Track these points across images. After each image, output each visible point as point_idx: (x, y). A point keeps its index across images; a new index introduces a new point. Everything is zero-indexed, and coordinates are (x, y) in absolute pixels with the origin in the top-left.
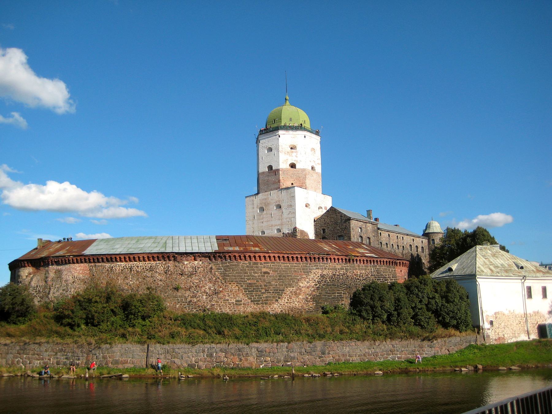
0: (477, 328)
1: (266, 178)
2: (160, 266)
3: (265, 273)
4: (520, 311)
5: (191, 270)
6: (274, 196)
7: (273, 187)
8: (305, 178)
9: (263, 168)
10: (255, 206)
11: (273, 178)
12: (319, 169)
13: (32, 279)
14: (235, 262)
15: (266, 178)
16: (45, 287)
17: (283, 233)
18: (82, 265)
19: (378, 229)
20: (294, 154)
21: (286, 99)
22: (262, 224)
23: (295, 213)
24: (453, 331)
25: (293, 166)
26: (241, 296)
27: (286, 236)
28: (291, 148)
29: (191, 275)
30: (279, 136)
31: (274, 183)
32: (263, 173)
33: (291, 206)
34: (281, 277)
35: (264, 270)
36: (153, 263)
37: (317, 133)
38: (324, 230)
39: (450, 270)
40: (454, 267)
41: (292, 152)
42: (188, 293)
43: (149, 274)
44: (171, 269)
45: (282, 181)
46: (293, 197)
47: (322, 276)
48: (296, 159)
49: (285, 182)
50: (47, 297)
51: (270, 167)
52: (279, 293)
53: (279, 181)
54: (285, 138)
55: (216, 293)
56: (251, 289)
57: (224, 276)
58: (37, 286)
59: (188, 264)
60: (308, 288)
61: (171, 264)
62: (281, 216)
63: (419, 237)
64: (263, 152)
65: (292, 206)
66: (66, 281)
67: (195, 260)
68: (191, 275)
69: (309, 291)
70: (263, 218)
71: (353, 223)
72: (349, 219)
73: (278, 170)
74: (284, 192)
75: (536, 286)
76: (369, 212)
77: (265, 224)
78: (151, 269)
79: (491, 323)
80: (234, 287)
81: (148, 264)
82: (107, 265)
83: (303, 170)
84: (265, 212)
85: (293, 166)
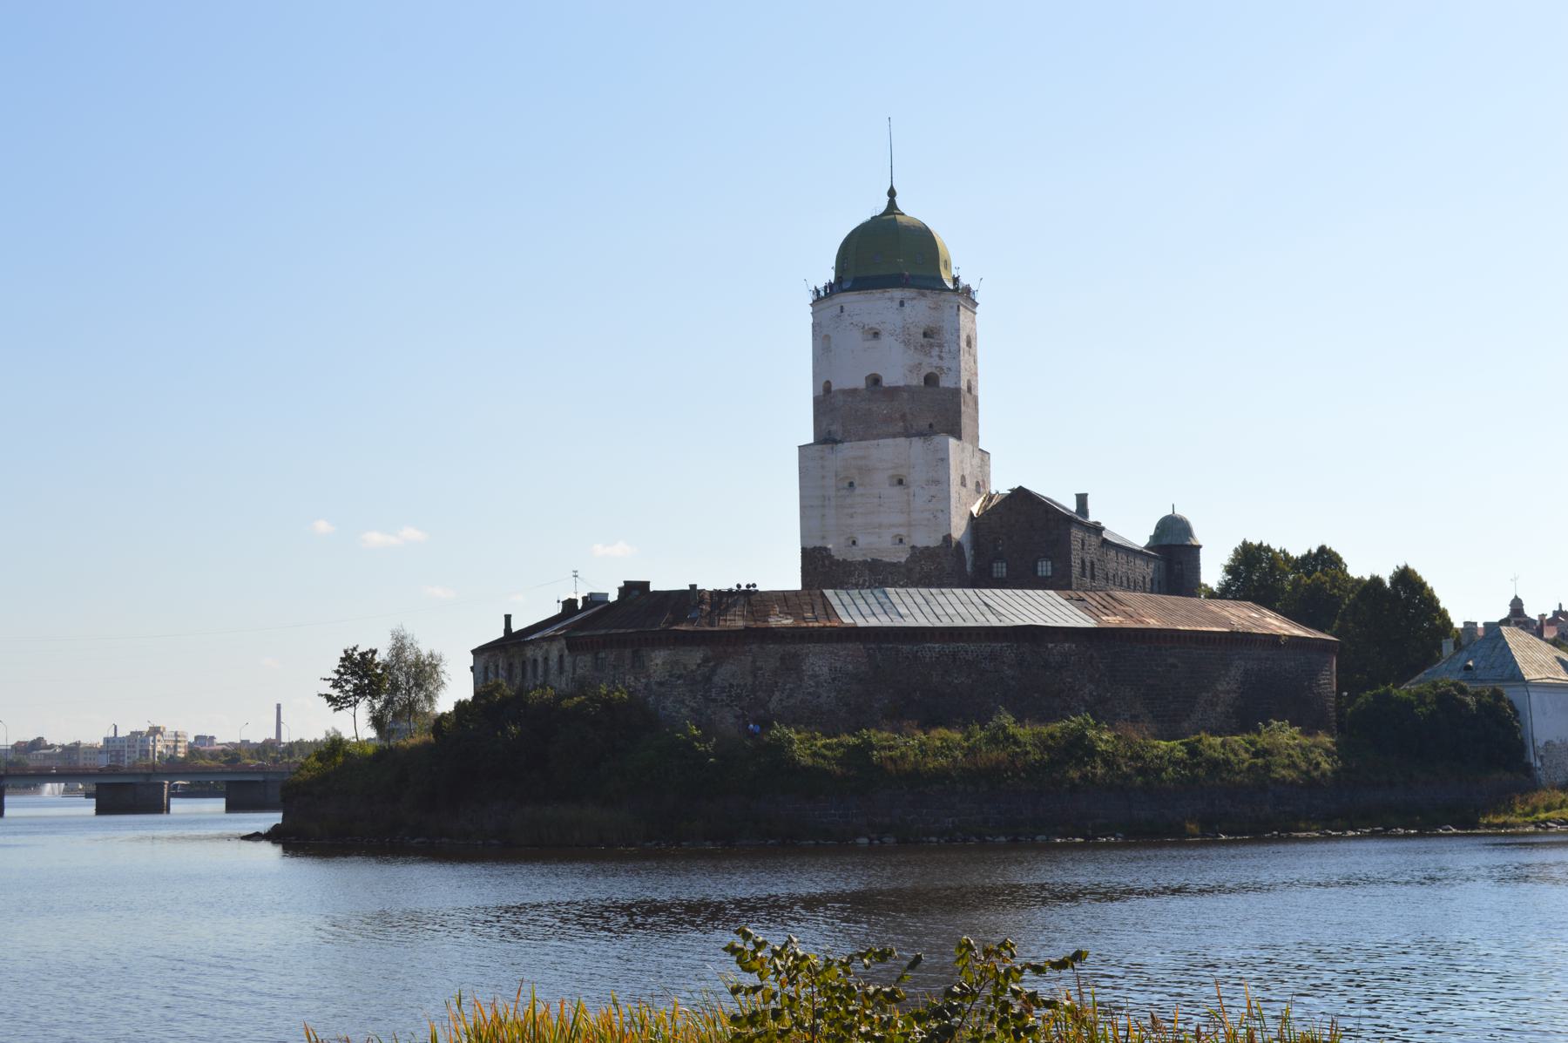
3: (1174, 666)
13: (713, 671)
17: (913, 547)
18: (850, 645)
19: (1105, 541)
20: (935, 351)
23: (948, 498)
25: (931, 380)
27: (919, 554)
30: (902, 304)
32: (854, 391)
33: (937, 482)
35: (1171, 660)
41: (932, 346)
46: (944, 460)
48: (940, 363)
51: (875, 380)
53: (903, 417)
60: (1228, 692)
65: (939, 482)
66: (815, 676)
76: (1082, 499)
79: (1541, 758)
82: (906, 648)
84: (859, 490)
85: (931, 380)
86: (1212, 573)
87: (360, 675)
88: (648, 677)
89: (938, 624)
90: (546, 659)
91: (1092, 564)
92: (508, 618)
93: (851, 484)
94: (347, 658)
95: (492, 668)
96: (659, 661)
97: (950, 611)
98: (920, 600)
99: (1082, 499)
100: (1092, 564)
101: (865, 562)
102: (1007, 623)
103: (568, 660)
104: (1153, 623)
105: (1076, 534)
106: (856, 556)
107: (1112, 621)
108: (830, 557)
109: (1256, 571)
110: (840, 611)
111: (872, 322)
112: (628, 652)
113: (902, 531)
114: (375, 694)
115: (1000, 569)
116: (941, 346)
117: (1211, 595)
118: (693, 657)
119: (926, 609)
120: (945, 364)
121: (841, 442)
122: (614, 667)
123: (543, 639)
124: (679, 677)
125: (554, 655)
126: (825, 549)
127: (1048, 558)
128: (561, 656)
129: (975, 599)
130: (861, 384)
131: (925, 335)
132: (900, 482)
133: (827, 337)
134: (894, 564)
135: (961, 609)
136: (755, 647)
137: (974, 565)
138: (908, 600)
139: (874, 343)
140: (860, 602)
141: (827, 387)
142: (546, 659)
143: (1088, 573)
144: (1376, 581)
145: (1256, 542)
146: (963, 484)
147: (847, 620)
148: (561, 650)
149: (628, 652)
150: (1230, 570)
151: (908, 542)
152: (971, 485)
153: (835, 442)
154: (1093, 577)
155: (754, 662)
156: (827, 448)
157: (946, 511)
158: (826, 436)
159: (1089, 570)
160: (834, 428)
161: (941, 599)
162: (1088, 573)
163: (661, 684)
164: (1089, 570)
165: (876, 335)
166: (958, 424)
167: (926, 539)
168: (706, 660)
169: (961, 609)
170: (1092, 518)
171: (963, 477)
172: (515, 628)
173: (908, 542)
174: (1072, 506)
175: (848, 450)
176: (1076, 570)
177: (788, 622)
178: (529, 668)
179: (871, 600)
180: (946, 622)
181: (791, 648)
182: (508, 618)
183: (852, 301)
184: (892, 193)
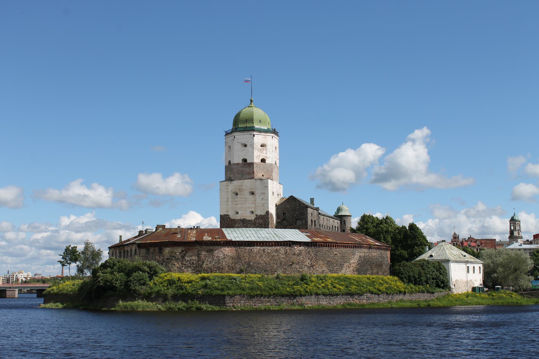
0: (450, 289)
1: (241, 169)
2: (282, 249)
3: (336, 254)
4: (465, 280)
5: (298, 252)
6: (247, 184)
7: (247, 176)
8: (272, 171)
9: (237, 160)
10: (230, 190)
11: (247, 170)
12: (278, 165)
14: (321, 248)
15: (241, 169)
16: (198, 261)
19: (319, 214)
20: (265, 151)
21: (251, 101)
22: (236, 206)
23: (267, 200)
24: (441, 290)
25: (263, 161)
26: (324, 268)
27: (258, 217)
28: (261, 146)
29: (299, 255)
31: (249, 173)
32: (238, 164)
34: (343, 257)
35: (335, 253)
36: (278, 248)
37: (274, 132)
38: (284, 213)
39: (431, 256)
40: (433, 254)
41: (263, 149)
42: (297, 266)
43: (276, 254)
44: (288, 251)
45: (255, 173)
46: (267, 187)
47: (360, 256)
48: (266, 155)
49: (258, 174)
50: (201, 266)
51: (245, 160)
52: (342, 266)
53: (253, 173)
54: (258, 139)
55: (312, 266)
56: (329, 264)
57: (316, 255)
58: (191, 260)
59: (297, 249)
61: (288, 248)
62: (255, 201)
63: (331, 218)
64: (237, 147)
67: (300, 246)
68: (299, 255)
69: (354, 265)
70: (237, 201)
71: (309, 209)
72: (307, 207)
73: (252, 164)
74: (258, 181)
75: (471, 266)
76: (312, 200)
77: (239, 206)
78: (277, 251)
80: (321, 262)
81: (274, 248)
83: (271, 165)
84: (239, 196)
85: (263, 161)
86: (354, 223)
87: (70, 255)
88: (163, 257)
89: (259, 240)
90: (131, 251)
91: (315, 221)
92: (121, 236)
93: (237, 194)
94: (67, 249)
95: (114, 253)
96: (167, 251)
97: (263, 236)
98: (254, 232)
99: (312, 200)
100: (315, 221)
101: (241, 219)
102: (282, 240)
103: (138, 251)
104: (329, 240)
105: (310, 210)
106: (238, 217)
107: (316, 239)
108: (230, 218)
109: (368, 225)
110: (227, 235)
111: (244, 142)
112: (157, 249)
113: (253, 210)
114: (75, 260)
115: (285, 223)
116: (266, 150)
117: (353, 231)
118: (178, 251)
119: (255, 235)
120: (268, 155)
121: (234, 180)
122: (153, 253)
123: (130, 244)
124: (174, 257)
125: (134, 249)
126: (228, 215)
127: (300, 219)
128: (136, 250)
129: (272, 233)
130: (241, 162)
131: (261, 146)
132: (253, 193)
133: (230, 147)
134: (250, 220)
135: (267, 235)
136: (198, 247)
137: (276, 221)
138: (250, 232)
139: (245, 148)
140: (234, 233)
141: (230, 162)
142: (131, 251)
143: (313, 224)
144: (404, 227)
145: (368, 215)
146: (273, 193)
147: (229, 238)
148: (135, 247)
149: (157, 249)
150: (359, 224)
151: (255, 213)
152: (276, 194)
153: (232, 180)
154: (315, 225)
155: (198, 252)
156: (229, 182)
157: (267, 203)
158: (229, 179)
159: (314, 222)
160: (231, 176)
161: (261, 232)
162: (313, 224)
163: (167, 259)
164: (314, 222)
165: (246, 146)
166: (272, 175)
167: (260, 212)
168: (182, 251)
169: (267, 235)
170: (316, 206)
171: (273, 193)
172: (123, 240)
173: (255, 213)
174: (309, 203)
175: (236, 183)
176: (309, 223)
177: (210, 239)
178: (126, 253)
179: (238, 232)
180: (261, 240)
181: (211, 248)
182: (121, 236)
183: (238, 135)
184: (251, 101)
